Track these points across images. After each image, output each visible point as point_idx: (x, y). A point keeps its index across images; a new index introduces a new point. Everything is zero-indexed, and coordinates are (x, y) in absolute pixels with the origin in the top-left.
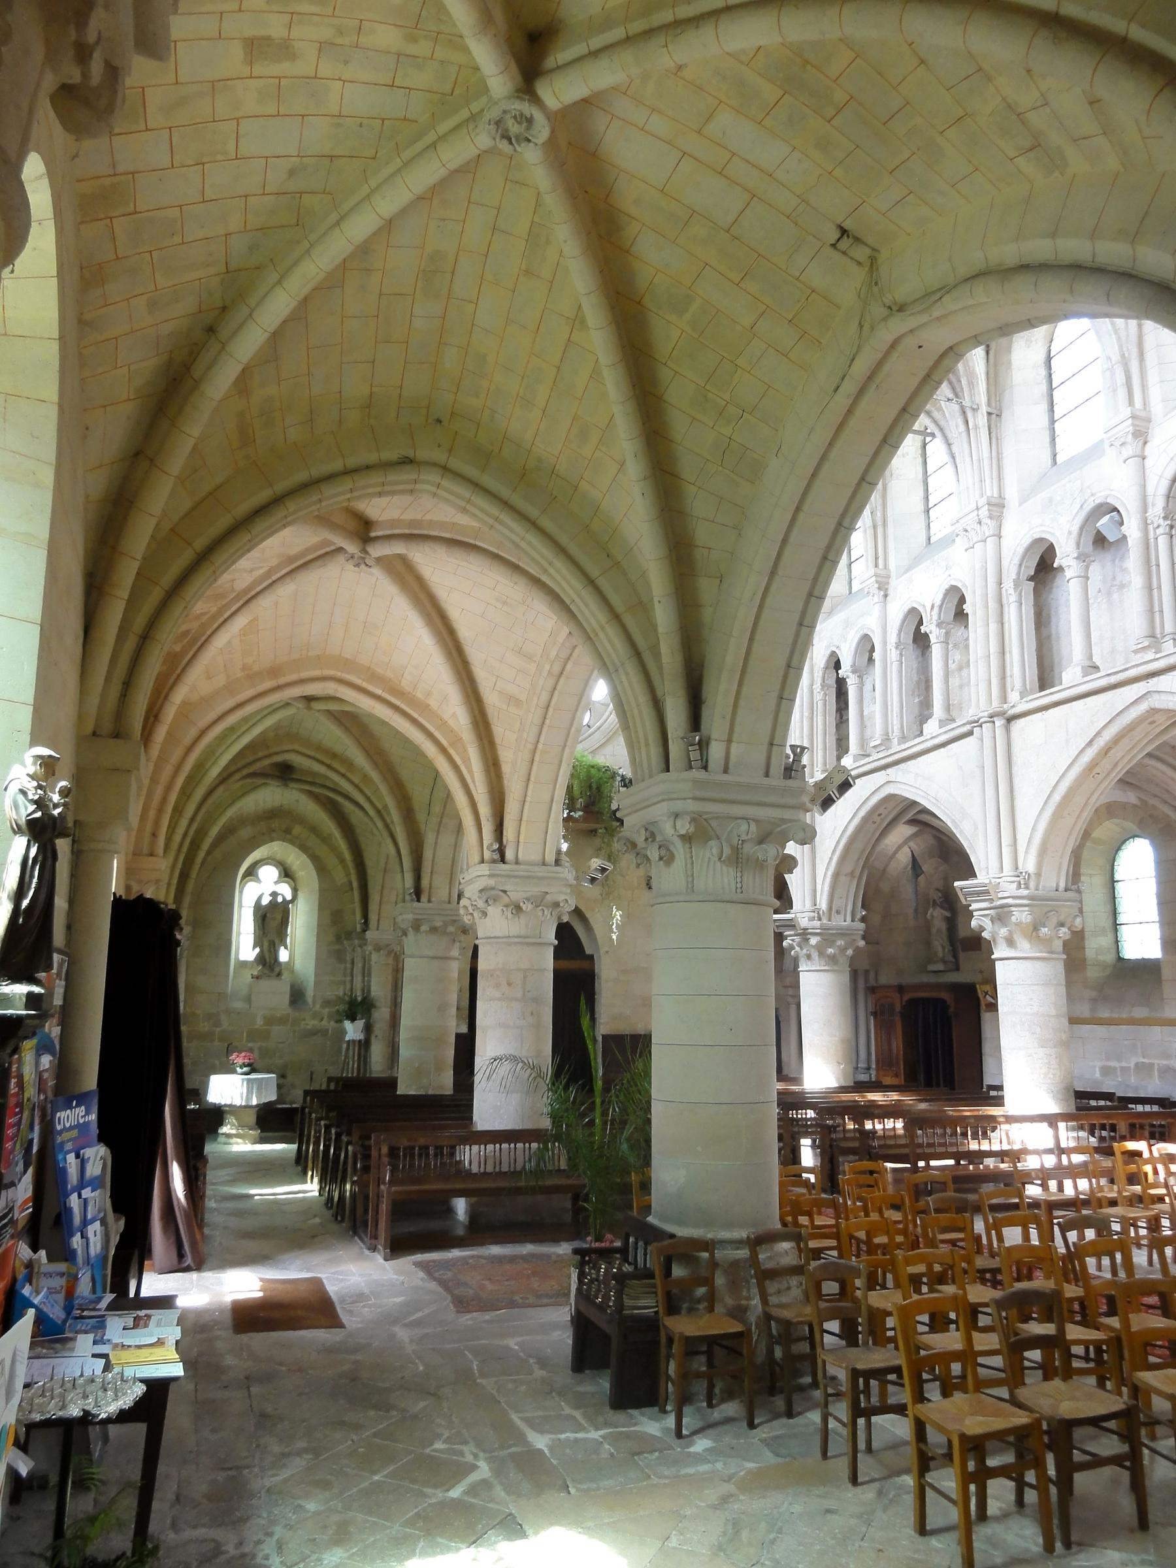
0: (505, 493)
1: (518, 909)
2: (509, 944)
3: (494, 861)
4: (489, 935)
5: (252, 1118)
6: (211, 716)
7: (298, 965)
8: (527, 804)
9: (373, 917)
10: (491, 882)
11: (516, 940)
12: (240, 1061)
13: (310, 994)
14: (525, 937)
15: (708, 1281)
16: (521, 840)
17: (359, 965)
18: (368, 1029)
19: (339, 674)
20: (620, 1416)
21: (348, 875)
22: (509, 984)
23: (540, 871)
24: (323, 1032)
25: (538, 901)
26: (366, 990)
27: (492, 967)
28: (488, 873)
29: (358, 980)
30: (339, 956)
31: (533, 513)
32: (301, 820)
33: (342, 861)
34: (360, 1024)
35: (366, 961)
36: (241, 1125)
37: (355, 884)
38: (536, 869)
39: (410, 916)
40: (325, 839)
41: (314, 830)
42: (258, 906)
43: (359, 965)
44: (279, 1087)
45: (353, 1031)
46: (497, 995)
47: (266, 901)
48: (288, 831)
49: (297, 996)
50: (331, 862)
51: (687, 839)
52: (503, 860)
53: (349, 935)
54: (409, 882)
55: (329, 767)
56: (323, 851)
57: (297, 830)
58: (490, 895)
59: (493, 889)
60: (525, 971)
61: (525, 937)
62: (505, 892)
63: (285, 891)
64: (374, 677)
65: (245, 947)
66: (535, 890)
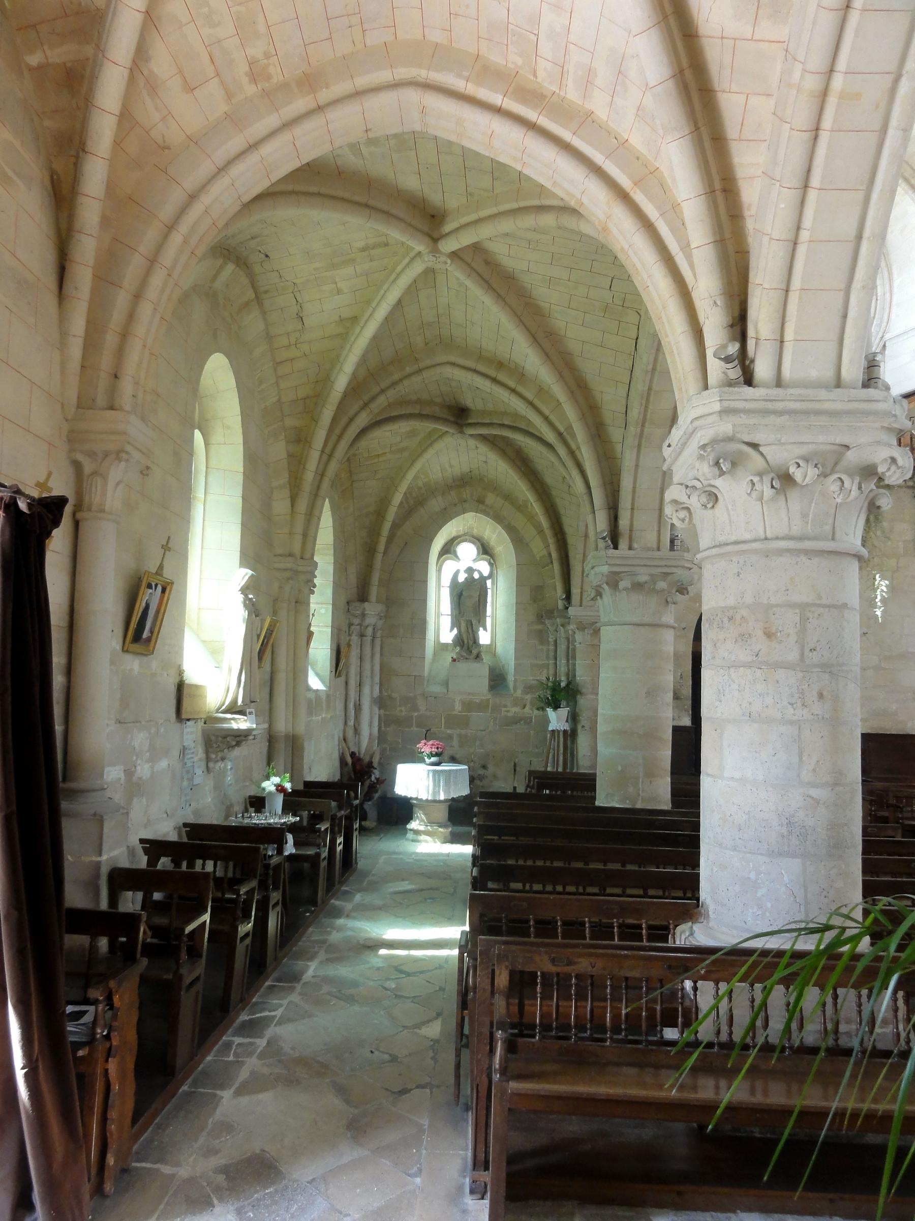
1: (787, 479)
2: (767, 554)
3: (730, 384)
4: (722, 539)
5: (442, 814)
6: (206, 168)
7: (499, 649)
8: (802, 250)
9: (575, 591)
10: (726, 427)
11: (783, 544)
12: (427, 750)
13: (511, 678)
14: (801, 539)
16: (789, 335)
17: (562, 647)
18: (574, 718)
19: (423, 74)
21: (547, 547)
22: (769, 635)
23: (834, 400)
24: (527, 721)
25: (829, 463)
26: (571, 674)
27: (731, 602)
28: (717, 407)
29: (562, 662)
30: (541, 636)
32: (492, 486)
33: (541, 531)
34: (564, 712)
35: (569, 641)
36: (431, 822)
37: (554, 555)
38: (823, 394)
39: (605, 569)
40: (521, 508)
41: (508, 497)
42: (454, 584)
43: (562, 647)
44: (472, 780)
45: (557, 720)
46: (744, 656)
47: (462, 578)
48: (481, 501)
49: (497, 680)
50: (529, 532)
52: (748, 379)
53: (550, 614)
54: (602, 523)
55: (494, 380)
56: (519, 521)
57: (491, 498)
58: (727, 457)
59: (730, 439)
60: (803, 607)
61: (801, 539)
62: (755, 446)
63: (484, 567)
64: (488, 72)
65: (441, 627)
66: (823, 439)
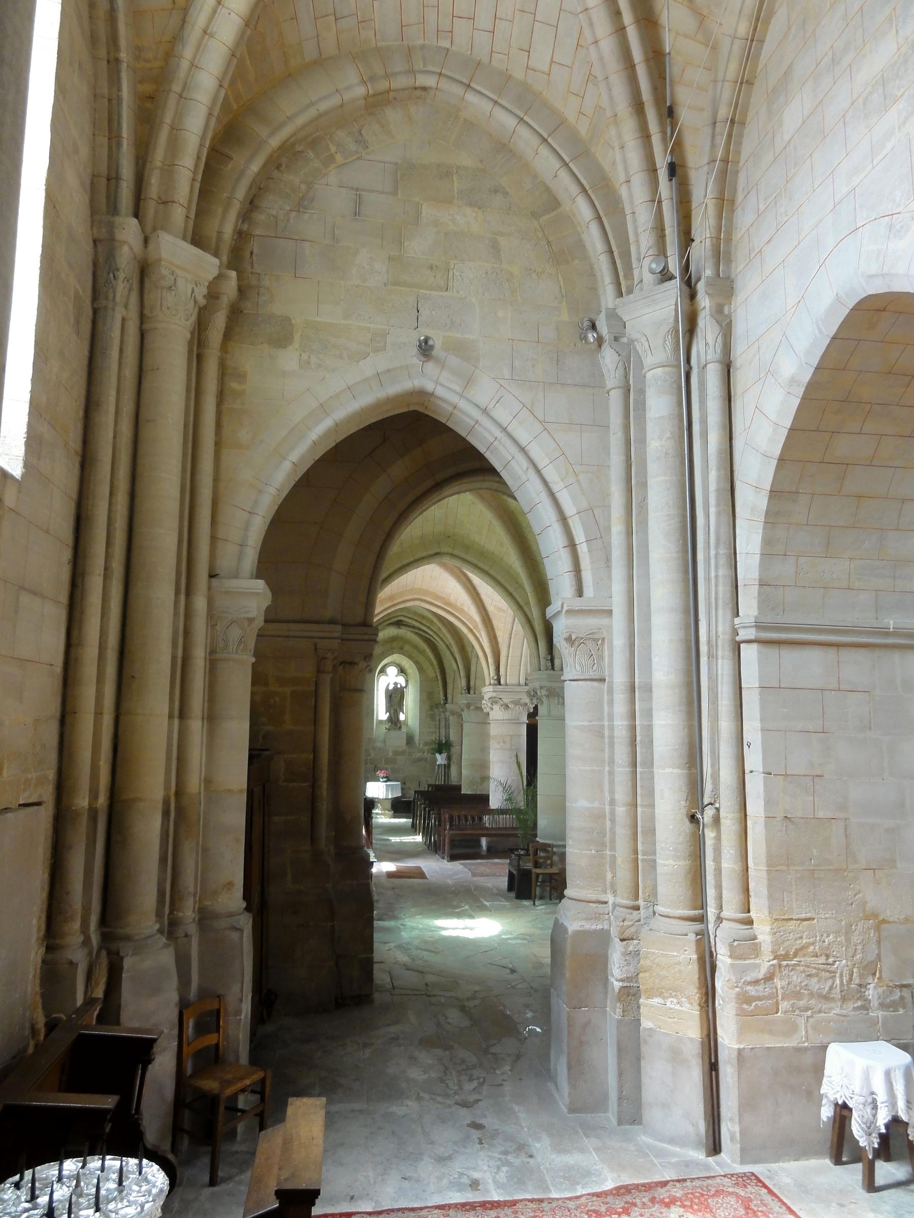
0: (475, 561)
3: (495, 685)
5: (389, 805)
7: (410, 722)
9: (449, 696)
10: (494, 694)
12: (381, 775)
13: (417, 739)
15: (551, 858)
17: (443, 723)
18: (449, 758)
19: (421, 597)
20: (518, 901)
21: (435, 672)
24: (425, 760)
25: (517, 703)
26: (447, 736)
29: (443, 731)
30: (432, 717)
31: (486, 568)
32: (408, 642)
33: (432, 665)
34: (444, 755)
35: (447, 720)
36: (384, 809)
37: (439, 678)
39: (465, 702)
40: (422, 652)
41: (416, 647)
42: (387, 690)
43: (443, 723)
44: (402, 789)
45: (440, 759)
47: (391, 687)
48: (401, 648)
49: (410, 740)
50: (426, 665)
51: (548, 696)
52: (499, 684)
53: (437, 706)
54: (464, 683)
55: (421, 623)
56: (421, 659)
57: (407, 647)
58: (494, 701)
63: (401, 681)
64: (438, 597)
65: (381, 712)
